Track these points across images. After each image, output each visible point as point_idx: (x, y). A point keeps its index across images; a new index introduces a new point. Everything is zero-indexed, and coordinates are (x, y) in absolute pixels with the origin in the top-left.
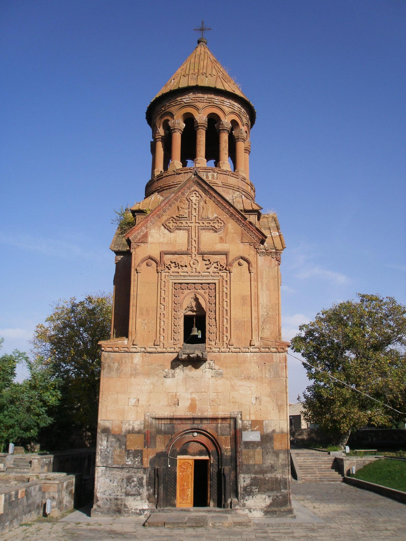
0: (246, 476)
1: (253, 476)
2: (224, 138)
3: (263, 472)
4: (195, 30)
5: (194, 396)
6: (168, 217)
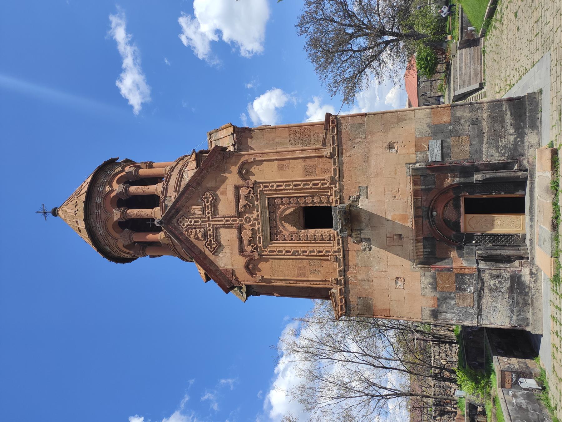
0: (485, 153)
1: (485, 146)
3: (481, 134)
4: (46, 220)
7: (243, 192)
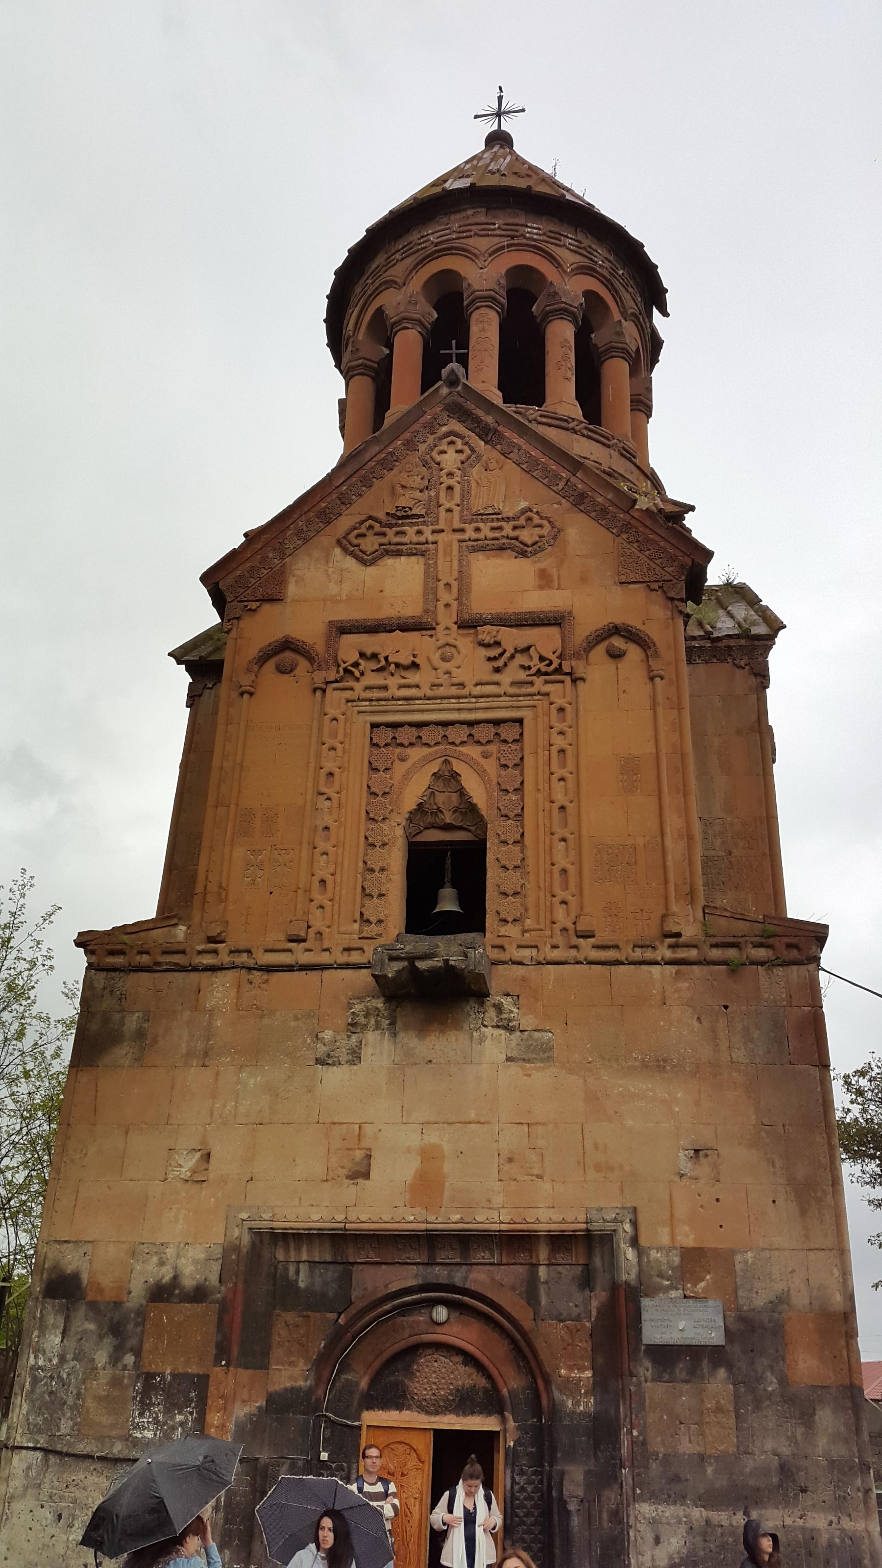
0: (669, 1512)
1: (697, 1514)
2: (561, 337)
5: (433, 1137)
6: (358, 520)
7: (547, 641)
